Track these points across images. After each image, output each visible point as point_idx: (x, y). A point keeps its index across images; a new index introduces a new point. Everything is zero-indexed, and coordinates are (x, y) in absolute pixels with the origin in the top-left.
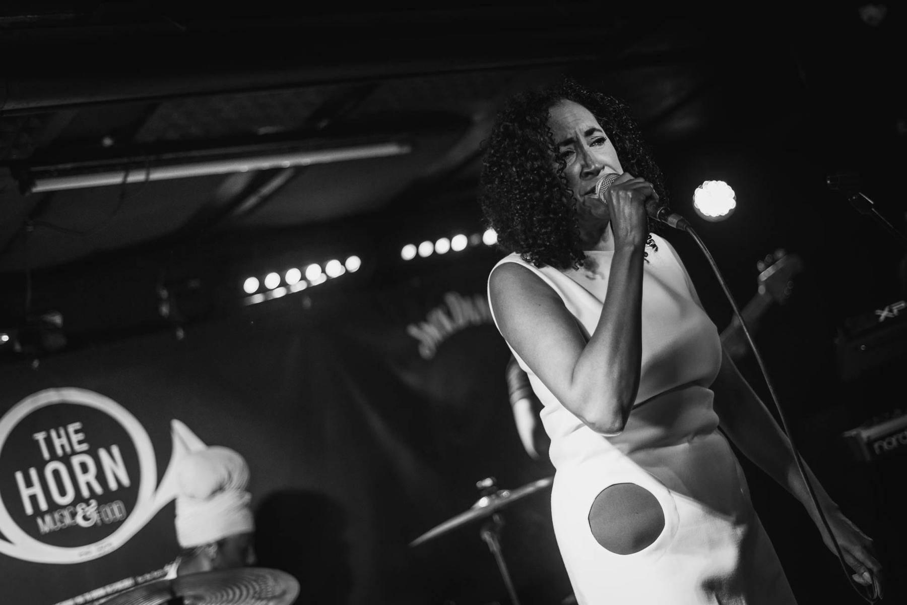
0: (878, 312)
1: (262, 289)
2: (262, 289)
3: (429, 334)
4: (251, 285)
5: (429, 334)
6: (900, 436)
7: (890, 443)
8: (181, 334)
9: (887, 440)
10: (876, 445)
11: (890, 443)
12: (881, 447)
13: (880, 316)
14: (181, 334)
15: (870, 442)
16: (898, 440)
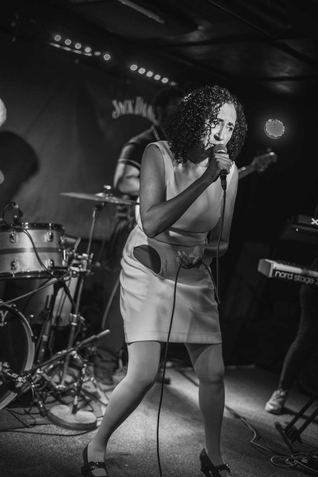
0: (313, 219)
1: (62, 43)
2: (62, 43)
3: (120, 108)
4: (58, 38)
5: (120, 108)
6: (288, 275)
7: (283, 275)
8: (14, 40)
9: (283, 273)
10: (277, 272)
11: (283, 275)
12: (278, 274)
13: (312, 221)
14: (14, 40)
15: (275, 271)
16: (287, 276)
